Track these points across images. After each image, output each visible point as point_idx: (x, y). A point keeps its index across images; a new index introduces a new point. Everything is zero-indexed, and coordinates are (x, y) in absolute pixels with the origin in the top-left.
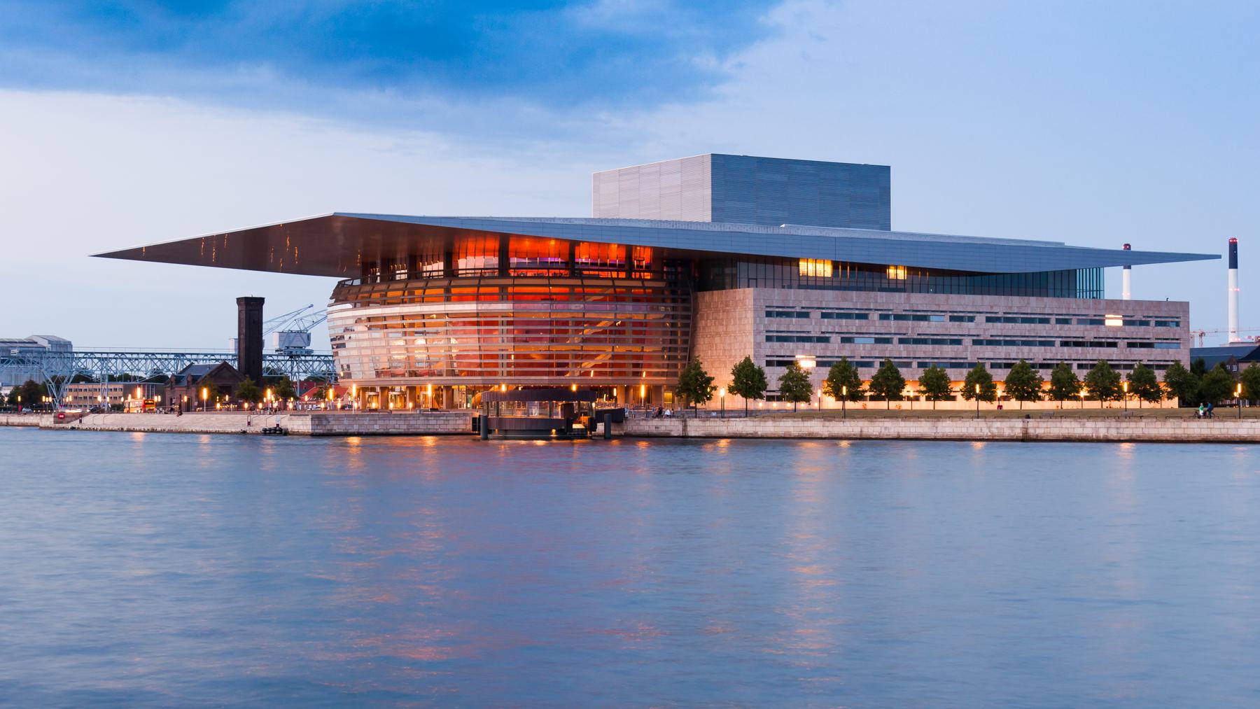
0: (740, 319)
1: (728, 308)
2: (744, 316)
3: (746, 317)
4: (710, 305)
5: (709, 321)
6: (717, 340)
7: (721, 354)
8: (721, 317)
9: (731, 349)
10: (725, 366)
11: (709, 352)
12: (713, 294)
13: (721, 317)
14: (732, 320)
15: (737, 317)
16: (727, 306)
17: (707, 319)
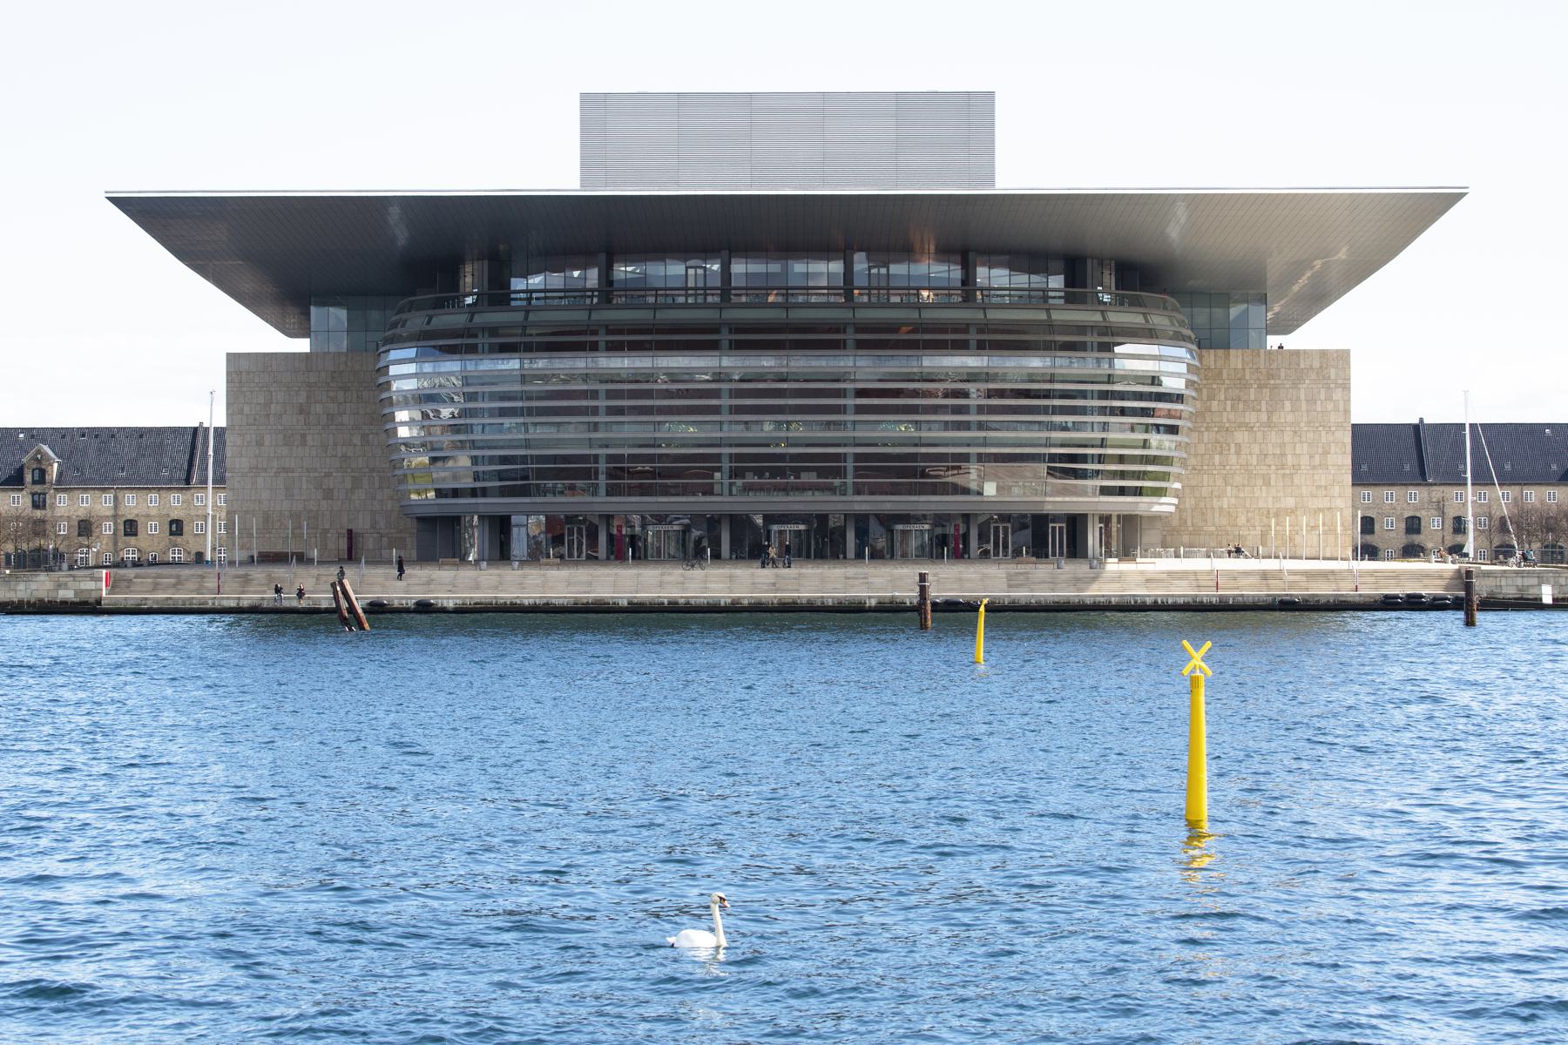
0: (1312, 401)
1: (1272, 382)
2: (1323, 396)
3: (1329, 398)
4: (1221, 373)
5: (1215, 403)
6: (1241, 436)
7: (1255, 463)
8: (1252, 397)
9: (1283, 455)
10: (1267, 483)
11: (1217, 457)
12: (1229, 353)
13: (1252, 397)
14: (1288, 404)
15: (1302, 397)
16: (1270, 376)
17: (1211, 398)
